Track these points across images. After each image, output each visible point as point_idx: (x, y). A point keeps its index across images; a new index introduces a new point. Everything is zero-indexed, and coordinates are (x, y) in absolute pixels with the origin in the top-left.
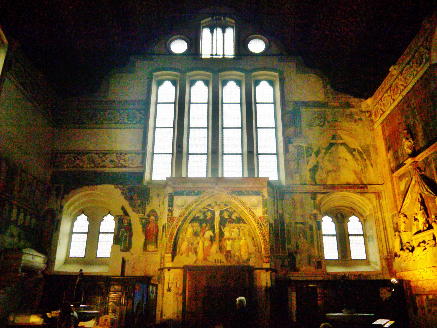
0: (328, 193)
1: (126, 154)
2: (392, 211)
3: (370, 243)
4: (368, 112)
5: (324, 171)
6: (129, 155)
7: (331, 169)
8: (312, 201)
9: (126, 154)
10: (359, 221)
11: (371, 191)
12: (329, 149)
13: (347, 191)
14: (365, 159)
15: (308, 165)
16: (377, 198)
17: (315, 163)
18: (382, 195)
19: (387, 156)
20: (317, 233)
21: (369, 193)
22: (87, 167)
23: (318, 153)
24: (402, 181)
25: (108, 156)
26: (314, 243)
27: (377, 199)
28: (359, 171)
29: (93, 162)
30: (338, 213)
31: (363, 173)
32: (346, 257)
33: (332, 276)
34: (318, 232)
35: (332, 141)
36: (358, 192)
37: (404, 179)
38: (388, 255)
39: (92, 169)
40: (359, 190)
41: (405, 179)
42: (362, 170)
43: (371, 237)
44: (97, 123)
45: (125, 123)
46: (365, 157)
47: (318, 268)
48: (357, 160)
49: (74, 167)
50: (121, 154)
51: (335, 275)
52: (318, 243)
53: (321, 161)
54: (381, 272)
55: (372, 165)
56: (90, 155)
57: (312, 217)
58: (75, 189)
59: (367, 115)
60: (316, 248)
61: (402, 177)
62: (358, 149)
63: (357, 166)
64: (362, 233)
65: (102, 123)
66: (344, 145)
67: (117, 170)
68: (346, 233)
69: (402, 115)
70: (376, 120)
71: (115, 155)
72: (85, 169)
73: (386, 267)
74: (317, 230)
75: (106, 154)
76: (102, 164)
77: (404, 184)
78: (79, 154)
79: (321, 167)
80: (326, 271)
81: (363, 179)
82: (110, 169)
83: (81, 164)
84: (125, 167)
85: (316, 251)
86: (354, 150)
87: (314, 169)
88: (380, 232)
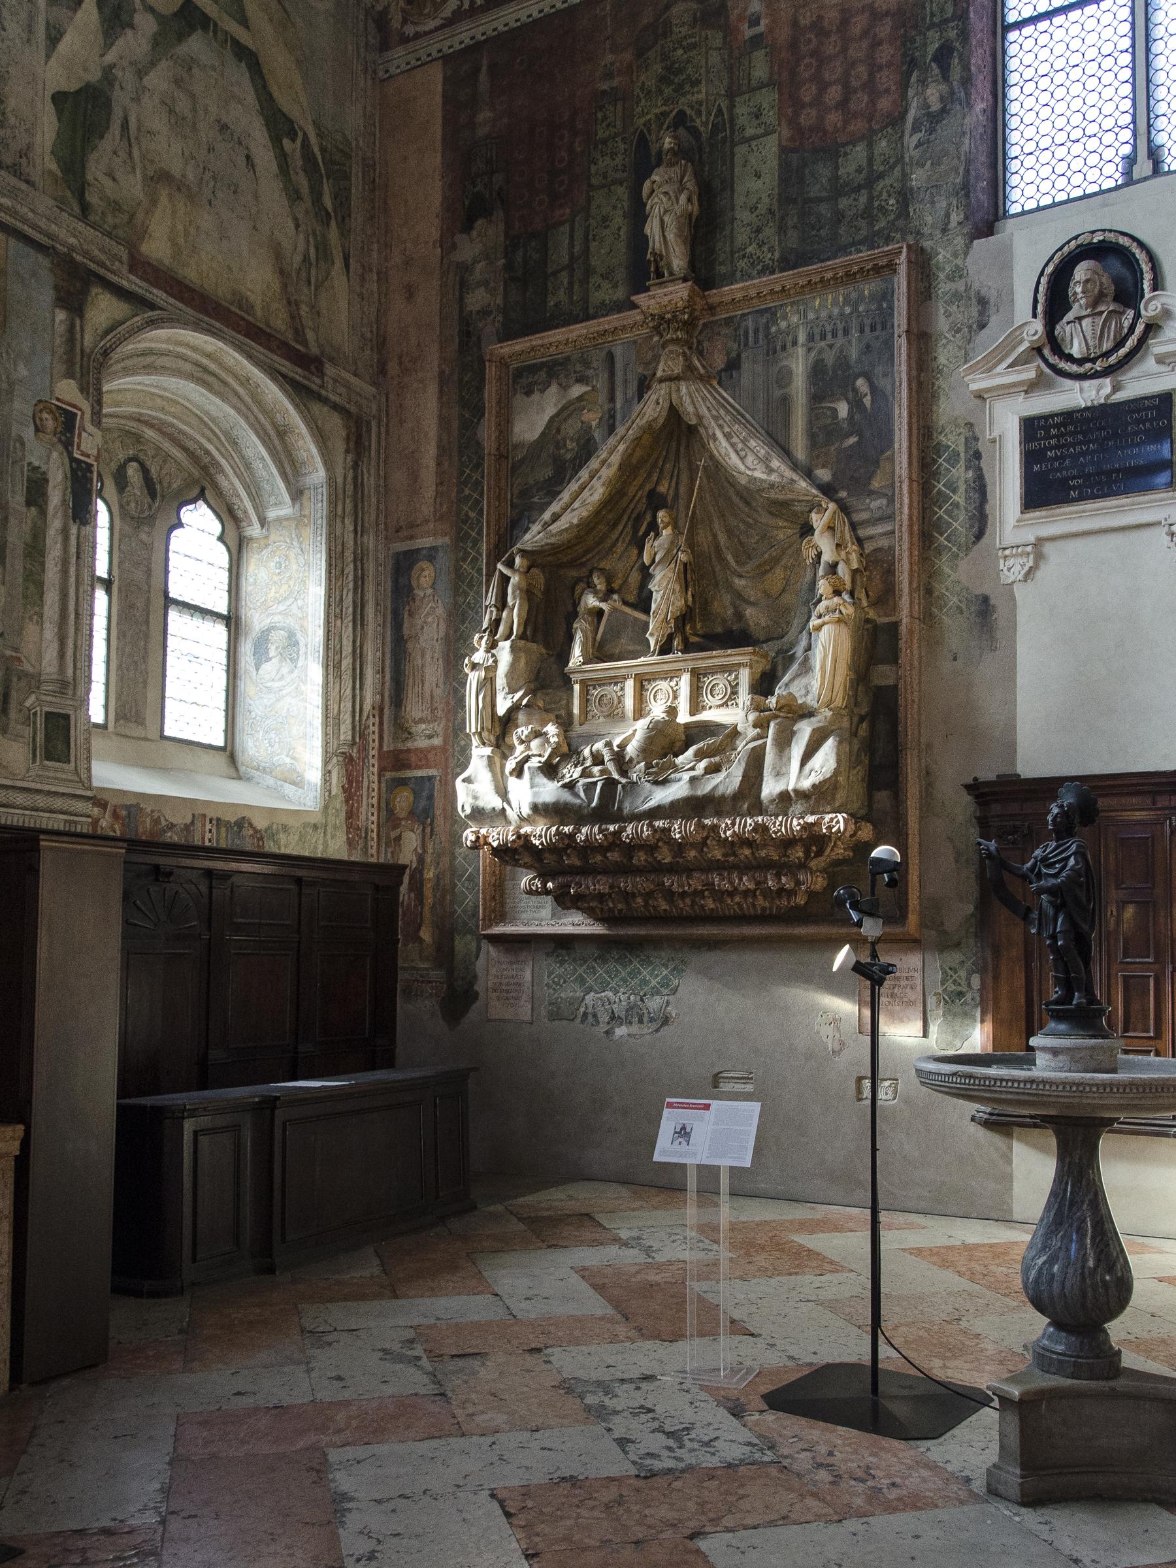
0: (152, 306)
2: (401, 534)
3: (266, 667)
5: (136, 153)
7: (176, 172)
8: (61, 315)
10: (221, 539)
11: (333, 397)
12: (181, 37)
13: (239, 348)
14: (328, 214)
15: (53, 62)
16: (352, 444)
17: (95, 76)
18: (370, 441)
19: (447, 245)
20: (65, 532)
21: (325, 401)
24: (536, 397)
26: (40, 586)
27: (347, 451)
28: (295, 266)
30: (130, 460)
31: (309, 283)
32: (140, 721)
33: (115, 815)
34: (74, 530)
36: (284, 376)
37: (553, 389)
38: (353, 743)
40: (286, 366)
41: (565, 388)
42: (306, 259)
43: (277, 637)
46: (328, 202)
47: (49, 756)
48: (294, 196)
51: (127, 807)
52: (64, 596)
53: (125, 76)
54: (318, 819)
55: (347, 266)
57: (50, 424)
60: (50, 633)
61: (543, 374)
62: (305, 134)
63: (291, 225)
64: (223, 610)
66: (249, 68)
68: (156, 582)
69: (640, 53)
70: (410, 30)
73: (341, 797)
74: (66, 515)
77: (550, 411)
79: (125, 125)
80: (90, 777)
81: (304, 309)
85: (50, 654)
88: (339, 622)
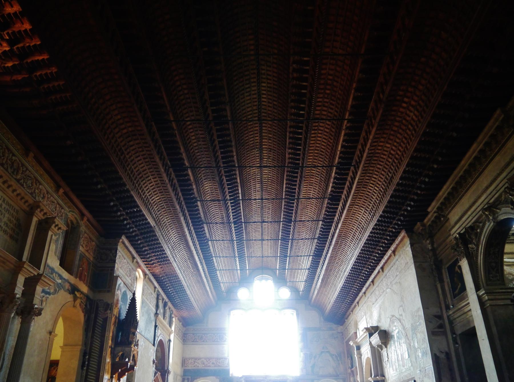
1: (220, 359)
4: (341, 333)
6: (222, 360)
9: (220, 359)
22: (201, 366)
23: (315, 357)
25: (211, 360)
29: (204, 364)
35: (323, 350)
39: (203, 368)
44: (203, 341)
45: (218, 341)
49: (194, 366)
50: (217, 359)
56: (202, 360)
58: (196, 379)
59: (341, 335)
65: (207, 342)
67: (216, 368)
71: (214, 360)
72: (200, 368)
75: (209, 359)
76: (208, 365)
78: (196, 359)
82: (212, 368)
83: (198, 365)
84: (219, 366)
86: (333, 355)
87: (313, 367)
